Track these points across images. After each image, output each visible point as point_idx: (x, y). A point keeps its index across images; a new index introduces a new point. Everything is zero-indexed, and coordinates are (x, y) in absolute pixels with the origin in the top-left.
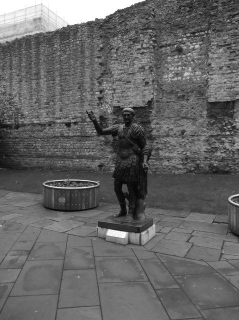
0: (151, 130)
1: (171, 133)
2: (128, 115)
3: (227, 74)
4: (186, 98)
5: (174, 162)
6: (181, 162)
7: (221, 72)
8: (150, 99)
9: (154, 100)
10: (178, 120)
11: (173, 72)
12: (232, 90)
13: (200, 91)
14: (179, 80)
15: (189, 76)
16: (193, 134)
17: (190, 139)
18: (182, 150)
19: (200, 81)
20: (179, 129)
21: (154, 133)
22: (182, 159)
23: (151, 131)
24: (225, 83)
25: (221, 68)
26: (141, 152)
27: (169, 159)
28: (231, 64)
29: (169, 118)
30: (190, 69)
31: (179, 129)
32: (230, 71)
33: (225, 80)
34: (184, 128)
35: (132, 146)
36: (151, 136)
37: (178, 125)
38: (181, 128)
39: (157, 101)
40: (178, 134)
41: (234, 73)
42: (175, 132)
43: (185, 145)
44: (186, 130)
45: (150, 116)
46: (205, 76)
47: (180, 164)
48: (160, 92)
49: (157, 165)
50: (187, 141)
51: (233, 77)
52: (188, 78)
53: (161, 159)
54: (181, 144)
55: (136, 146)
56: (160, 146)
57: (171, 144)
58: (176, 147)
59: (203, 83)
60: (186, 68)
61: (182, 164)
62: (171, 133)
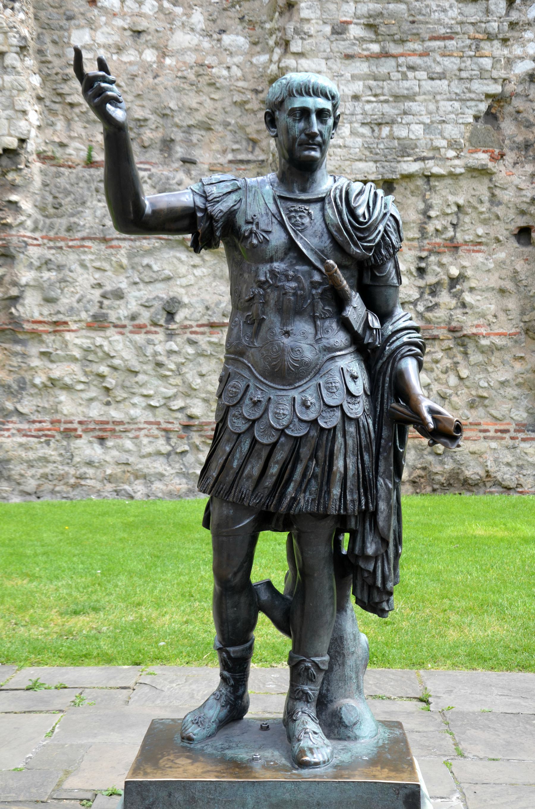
0: (14, 292)
1: (120, 312)
2: (321, 114)
3: (367, 58)
4: (180, 151)
5: (128, 444)
6: (162, 446)
7: (342, 46)
8: (13, 143)
9: (31, 146)
10: (149, 252)
11: (119, 22)
12: (385, 131)
13: (242, 128)
14: (147, 67)
15: (197, 49)
16: (215, 319)
17: (202, 340)
18: (171, 392)
19: (244, 78)
20: (146, 293)
21: (31, 308)
22: (166, 431)
23: (15, 300)
24: (356, 97)
25: (339, 30)
26: (387, 340)
27: (103, 432)
28: (380, 14)
29: (104, 240)
30: (198, 18)
31: (146, 293)
32: (375, 48)
33: (358, 87)
34: (177, 290)
35: (340, 302)
36: (16, 322)
37: (147, 275)
38: (161, 291)
39: (42, 157)
40: (145, 317)
41: (395, 57)
42: (133, 306)
43: (180, 365)
44: (186, 300)
45: (8, 226)
46: (264, 58)
47: (159, 453)
48: (54, 113)
49: (45, 460)
50: (190, 350)
51: (388, 77)
52: (191, 58)
53: (69, 434)
54: (159, 365)
55: (356, 310)
56: (58, 371)
57: (117, 362)
58: (141, 378)
59: (256, 92)
60: (179, 10)
61: (168, 455)
62: (120, 312)
